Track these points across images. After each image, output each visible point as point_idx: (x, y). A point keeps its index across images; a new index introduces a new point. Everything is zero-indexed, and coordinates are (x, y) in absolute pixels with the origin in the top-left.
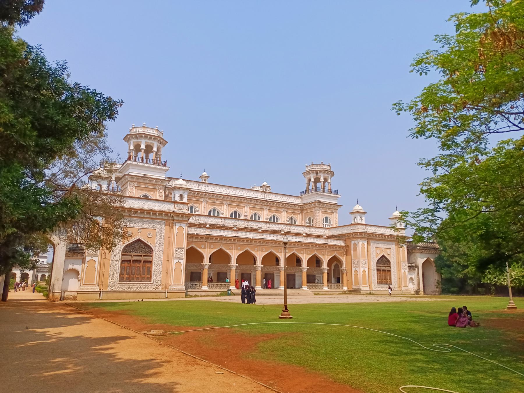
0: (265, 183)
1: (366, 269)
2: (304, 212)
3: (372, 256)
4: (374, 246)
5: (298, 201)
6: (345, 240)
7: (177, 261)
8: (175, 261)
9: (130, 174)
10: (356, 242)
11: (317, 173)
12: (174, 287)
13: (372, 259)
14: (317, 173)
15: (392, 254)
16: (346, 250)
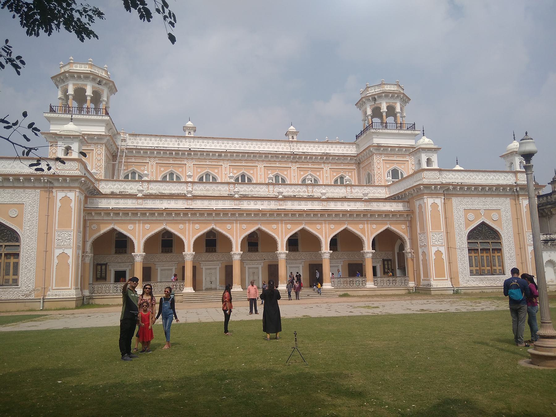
0: (292, 127)
1: (443, 249)
2: (362, 166)
3: (456, 226)
4: (460, 205)
5: (351, 150)
6: (408, 202)
7: (61, 251)
8: (58, 252)
9: (51, 132)
10: (421, 202)
11: (375, 100)
12: (57, 292)
13: (457, 231)
14: (375, 100)
15: (504, 219)
16: (410, 217)
